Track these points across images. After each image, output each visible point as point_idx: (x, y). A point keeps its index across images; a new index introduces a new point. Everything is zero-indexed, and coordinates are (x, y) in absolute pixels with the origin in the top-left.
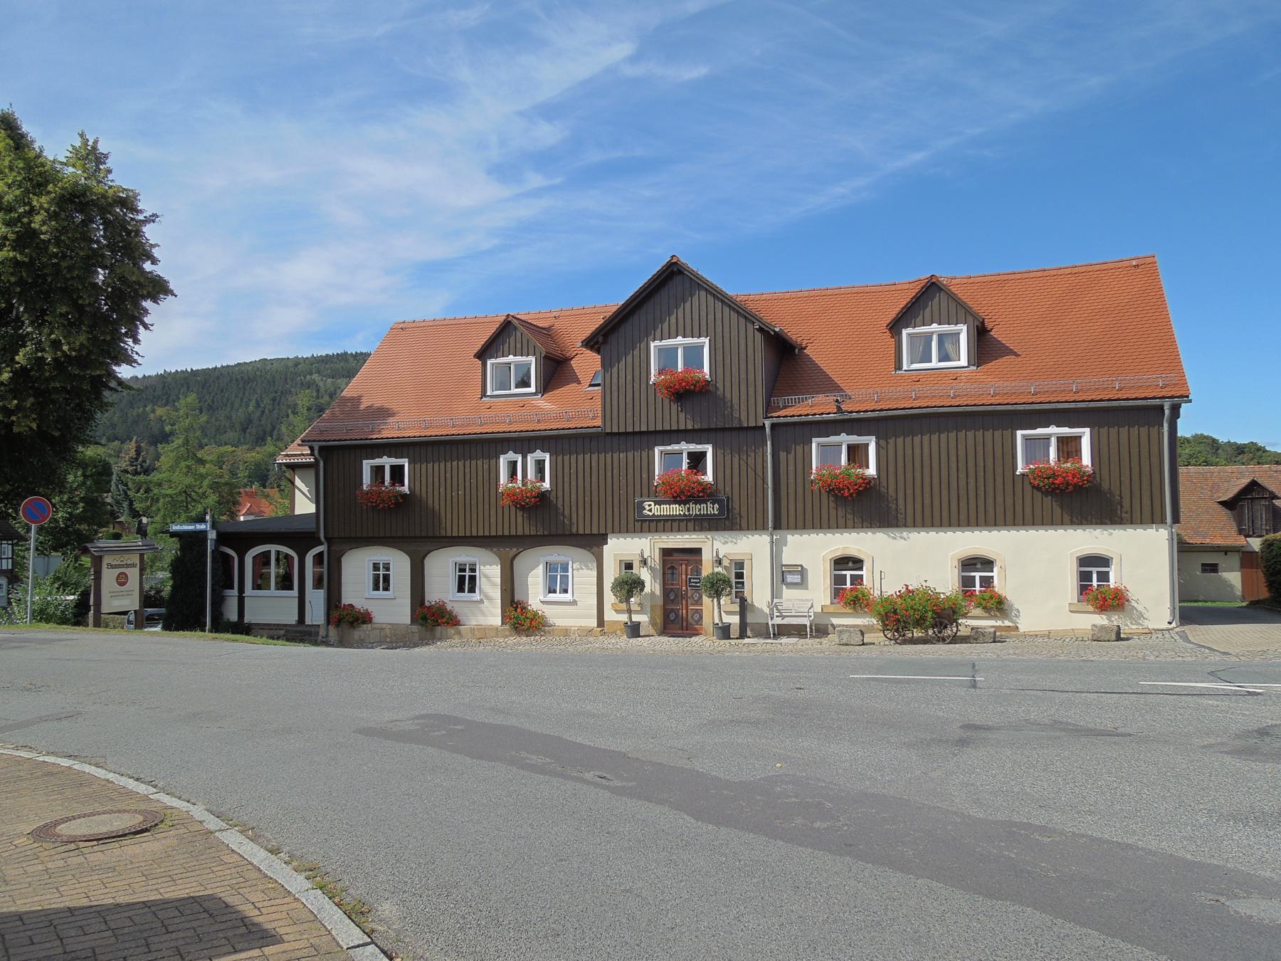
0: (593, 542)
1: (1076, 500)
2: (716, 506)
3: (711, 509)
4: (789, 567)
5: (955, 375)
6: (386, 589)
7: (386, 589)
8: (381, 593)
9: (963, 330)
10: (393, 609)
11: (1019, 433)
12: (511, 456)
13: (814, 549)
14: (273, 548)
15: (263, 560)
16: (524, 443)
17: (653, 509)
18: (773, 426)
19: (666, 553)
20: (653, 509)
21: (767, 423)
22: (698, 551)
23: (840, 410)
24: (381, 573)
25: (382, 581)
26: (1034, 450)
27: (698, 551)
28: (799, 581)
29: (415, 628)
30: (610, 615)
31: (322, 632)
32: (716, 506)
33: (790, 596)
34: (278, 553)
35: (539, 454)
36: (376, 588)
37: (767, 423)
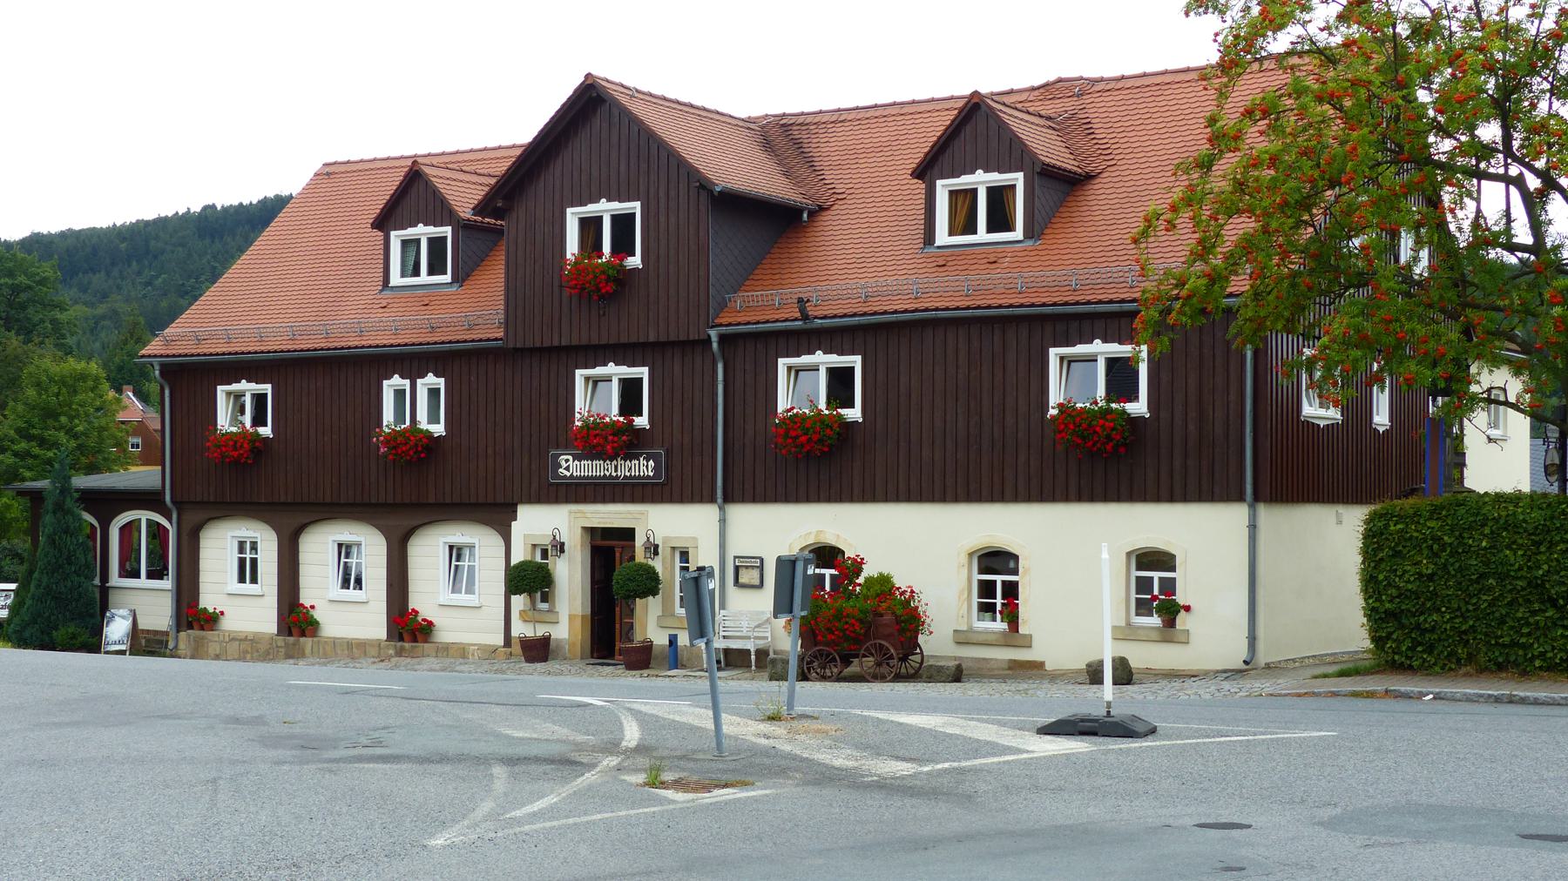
1: (1098, 462)
2: (651, 463)
3: (643, 468)
6: (254, 580)
7: (254, 580)
8: (248, 587)
12: (396, 380)
13: (777, 530)
14: (144, 516)
15: (129, 530)
16: (412, 362)
17: (572, 467)
18: (723, 339)
19: (592, 532)
20: (572, 467)
21: (713, 333)
22: (629, 534)
23: (805, 317)
24: (248, 556)
25: (247, 571)
26: (1073, 379)
27: (629, 534)
28: (757, 582)
29: (281, 641)
31: (171, 645)
32: (651, 463)
35: (431, 380)
36: (242, 579)
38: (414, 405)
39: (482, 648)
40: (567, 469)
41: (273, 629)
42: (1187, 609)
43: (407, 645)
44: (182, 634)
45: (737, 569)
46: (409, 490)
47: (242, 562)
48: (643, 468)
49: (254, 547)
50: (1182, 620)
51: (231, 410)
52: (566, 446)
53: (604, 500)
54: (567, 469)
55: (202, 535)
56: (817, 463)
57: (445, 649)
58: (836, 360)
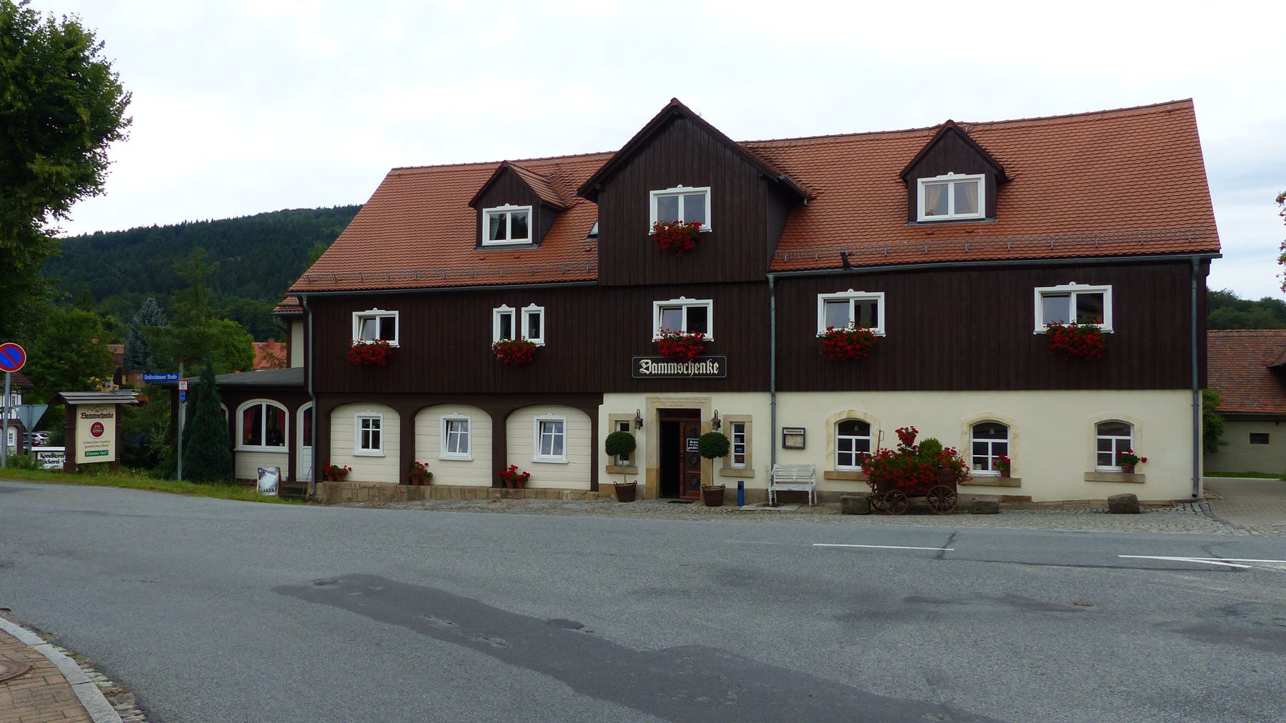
0: (589, 404)
2: (716, 365)
3: (711, 368)
5: (514, 252)
6: (376, 446)
7: (376, 446)
10: (381, 467)
12: (504, 308)
13: (818, 412)
14: (264, 403)
15: (254, 414)
16: (518, 296)
17: (649, 367)
18: (776, 280)
19: (662, 412)
20: (649, 367)
21: (771, 276)
22: (696, 413)
23: (846, 265)
24: (371, 430)
25: (371, 439)
27: (696, 413)
29: (404, 488)
30: (604, 478)
31: (310, 491)
32: (716, 365)
34: (268, 407)
35: (533, 307)
36: (365, 446)
37: (771, 276)
39: (573, 491)
40: (647, 369)
41: (397, 479)
42: (1144, 460)
43: (511, 490)
44: (320, 485)
45: (784, 436)
46: (507, 385)
47: (366, 435)
48: (711, 368)
49: (376, 423)
50: (1139, 469)
51: (364, 330)
52: (646, 354)
54: (647, 369)
55: (333, 415)
56: (849, 364)
57: (543, 493)
58: (693, 302)
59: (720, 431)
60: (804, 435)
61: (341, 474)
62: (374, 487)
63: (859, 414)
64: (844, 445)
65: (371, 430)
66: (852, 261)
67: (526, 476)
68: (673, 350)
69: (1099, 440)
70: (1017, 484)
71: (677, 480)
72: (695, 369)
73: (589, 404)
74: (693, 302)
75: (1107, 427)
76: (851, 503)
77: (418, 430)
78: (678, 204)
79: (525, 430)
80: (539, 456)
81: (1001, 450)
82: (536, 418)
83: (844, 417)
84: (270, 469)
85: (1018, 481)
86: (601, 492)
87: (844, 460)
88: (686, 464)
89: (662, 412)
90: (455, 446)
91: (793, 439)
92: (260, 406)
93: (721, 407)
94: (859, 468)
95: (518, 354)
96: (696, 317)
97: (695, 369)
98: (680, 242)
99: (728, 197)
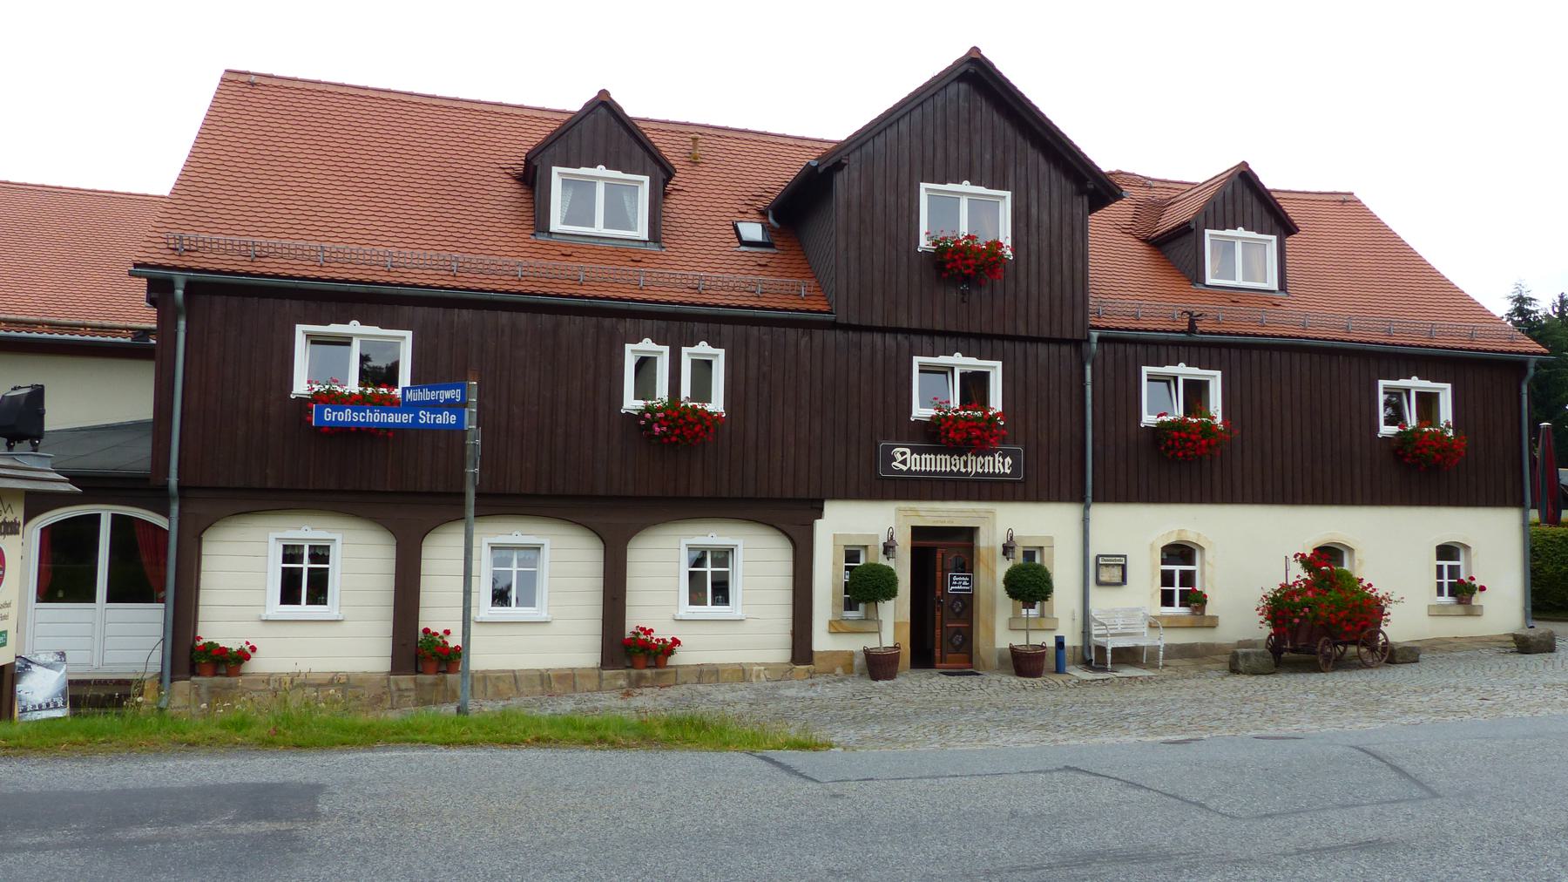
0: (793, 519)
2: (1008, 460)
3: (1000, 465)
4: (1101, 556)
8: (303, 610)
9: (556, 225)
10: (344, 638)
11: (1382, 383)
13: (1137, 530)
16: (678, 323)
17: (907, 460)
18: (1100, 339)
19: (917, 532)
20: (907, 460)
21: (1095, 334)
22: (970, 533)
23: (1192, 328)
27: (970, 533)
28: (1118, 579)
29: (406, 681)
30: (822, 641)
33: (1102, 601)
34: (116, 519)
35: (703, 349)
37: (1095, 334)
38: (662, 376)
39: (767, 666)
40: (904, 462)
41: (384, 665)
42: (1483, 589)
43: (648, 672)
44: (182, 685)
45: (1098, 565)
48: (1000, 465)
49: (320, 554)
50: (1478, 599)
51: (321, 364)
52: (901, 439)
53: (932, 497)
54: (904, 462)
55: (204, 536)
56: (1179, 467)
59: (891, 564)
60: (1124, 567)
61: (228, 662)
62: (331, 683)
63: (1190, 536)
64: (1167, 578)
65: (709, 569)
66: (1200, 326)
67: (669, 648)
68: (934, 436)
69: (1191, 562)
70: (1212, 624)
71: (941, 637)
72: (977, 465)
73: (793, 519)
74: (973, 363)
75: (1447, 551)
76: (1253, 659)
77: (426, 566)
78: (967, 211)
79: (661, 561)
80: (687, 610)
81: (1187, 578)
82: (273, 535)
83: (1172, 540)
84: (42, 658)
85: (1214, 619)
86: (818, 665)
87: (1167, 599)
88: (938, 612)
89: (917, 532)
90: (521, 596)
91: (1108, 571)
92: (96, 519)
93: (1005, 524)
94: (1184, 611)
95: (677, 429)
96: (974, 385)
97: (977, 465)
98: (961, 266)
99: (1034, 211)
